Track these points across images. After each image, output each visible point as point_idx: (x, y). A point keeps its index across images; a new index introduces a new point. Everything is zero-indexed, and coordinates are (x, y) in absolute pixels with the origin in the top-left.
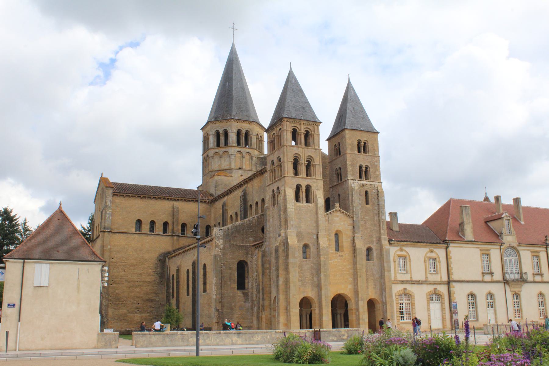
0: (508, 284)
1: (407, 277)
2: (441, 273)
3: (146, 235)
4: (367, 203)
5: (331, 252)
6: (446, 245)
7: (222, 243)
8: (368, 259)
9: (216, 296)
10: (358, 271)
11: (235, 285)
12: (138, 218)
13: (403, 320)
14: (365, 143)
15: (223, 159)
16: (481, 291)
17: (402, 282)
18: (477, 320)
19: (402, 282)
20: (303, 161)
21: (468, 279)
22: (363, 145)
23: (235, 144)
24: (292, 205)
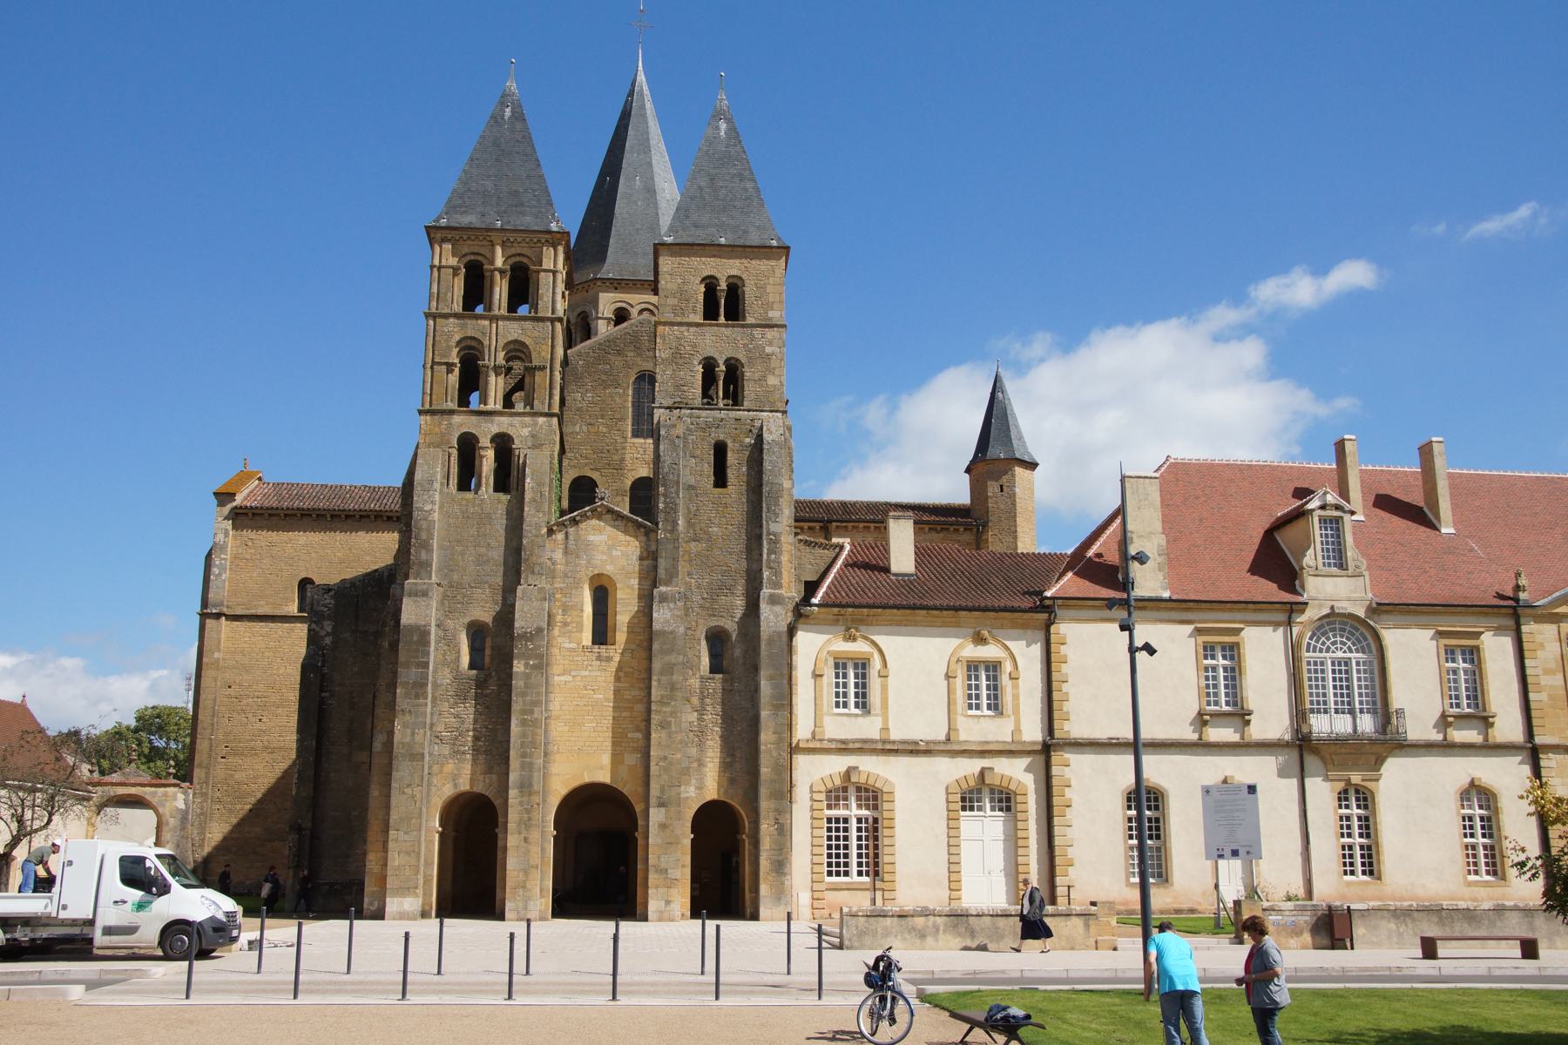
0: (1315, 751)
1: (868, 728)
2: (1016, 711)
4: (720, 480)
5: (567, 645)
6: (1045, 616)
7: (329, 630)
9: (298, 788)
10: (653, 707)
12: (304, 575)
13: (846, 874)
17: (844, 748)
18: (1167, 881)
19: (844, 748)
20: (495, 356)
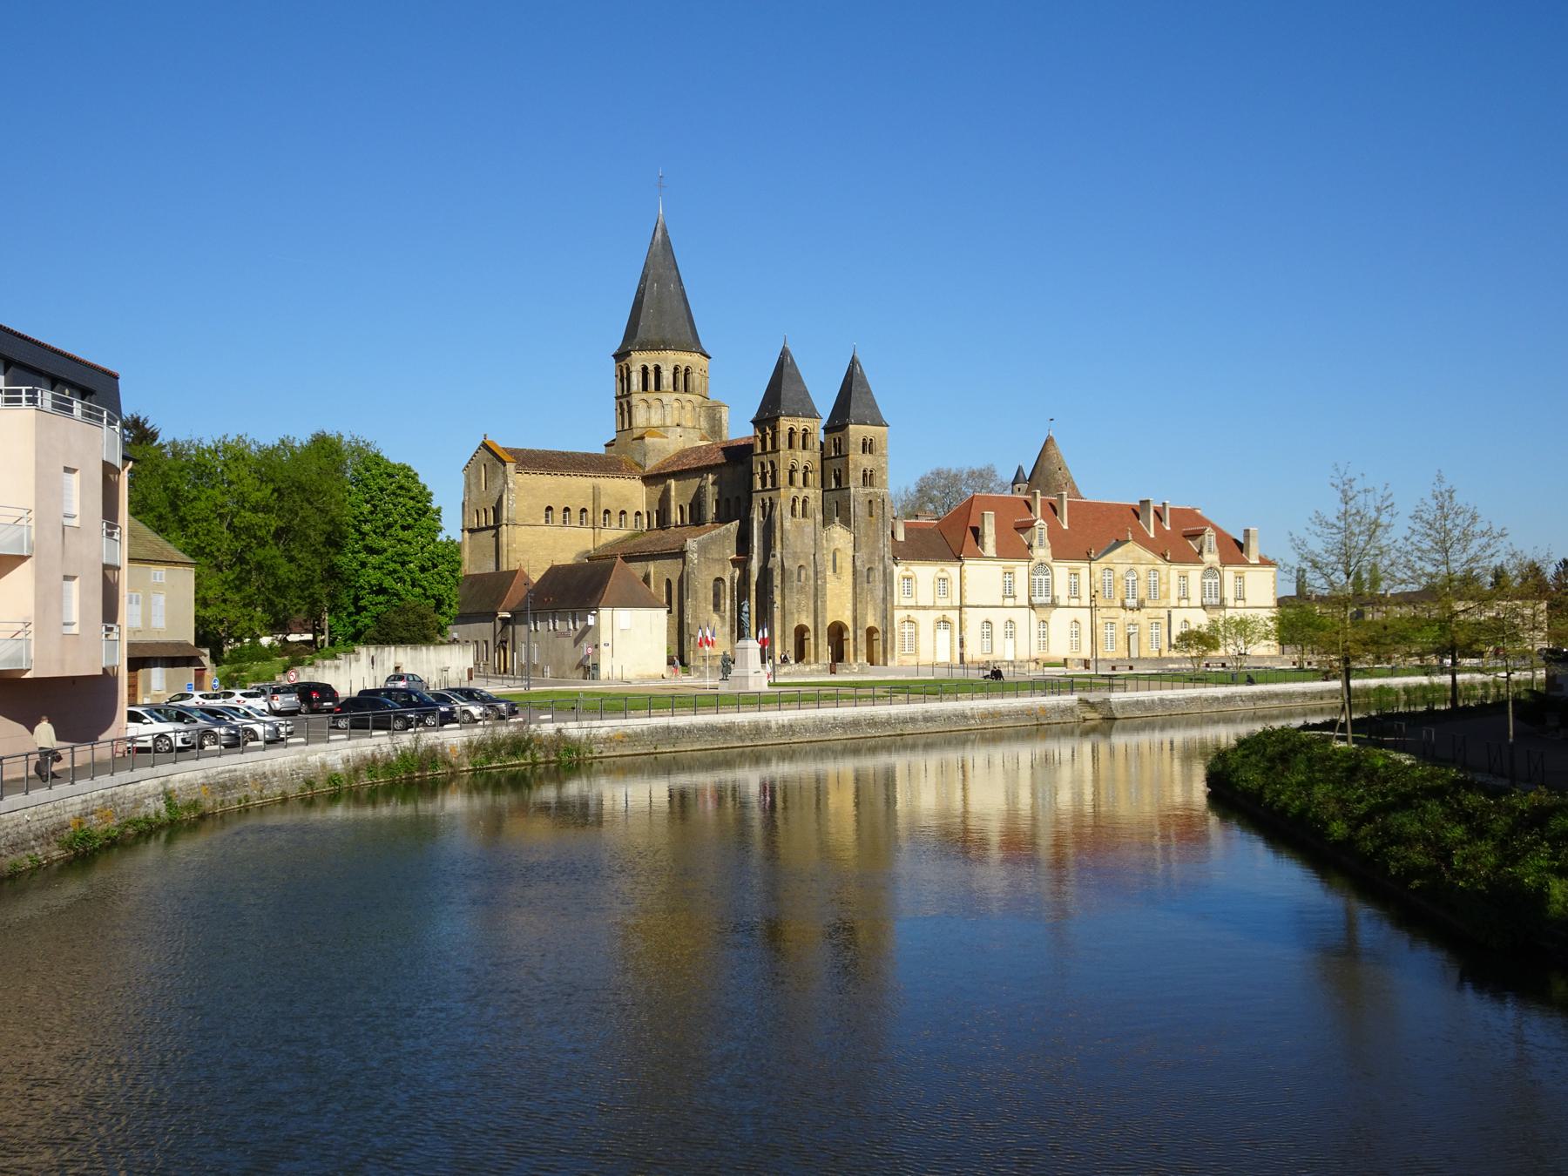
1: (911, 602)
4: (871, 516)
8: (868, 582)
11: (711, 607)
14: (871, 440)
15: (653, 411)
16: (998, 617)
17: (906, 607)
19: (906, 607)
21: (984, 604)
22: (868, 443)
23: (671, 389)
24: (787, 525)
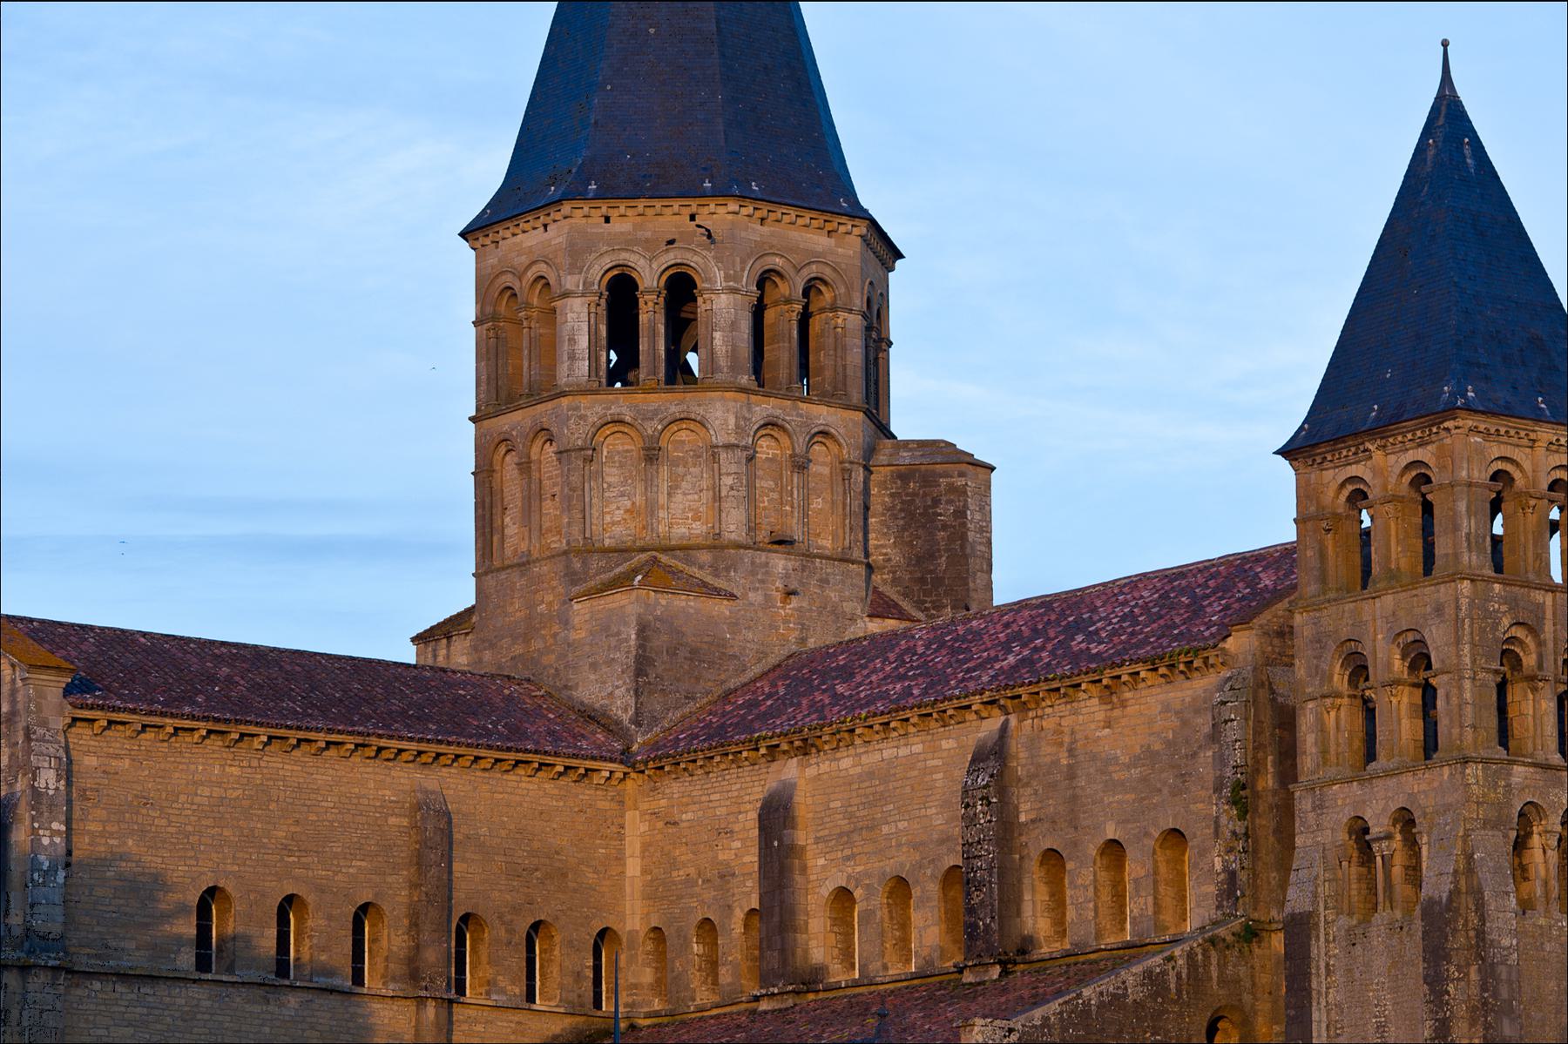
3: (260, 992)
